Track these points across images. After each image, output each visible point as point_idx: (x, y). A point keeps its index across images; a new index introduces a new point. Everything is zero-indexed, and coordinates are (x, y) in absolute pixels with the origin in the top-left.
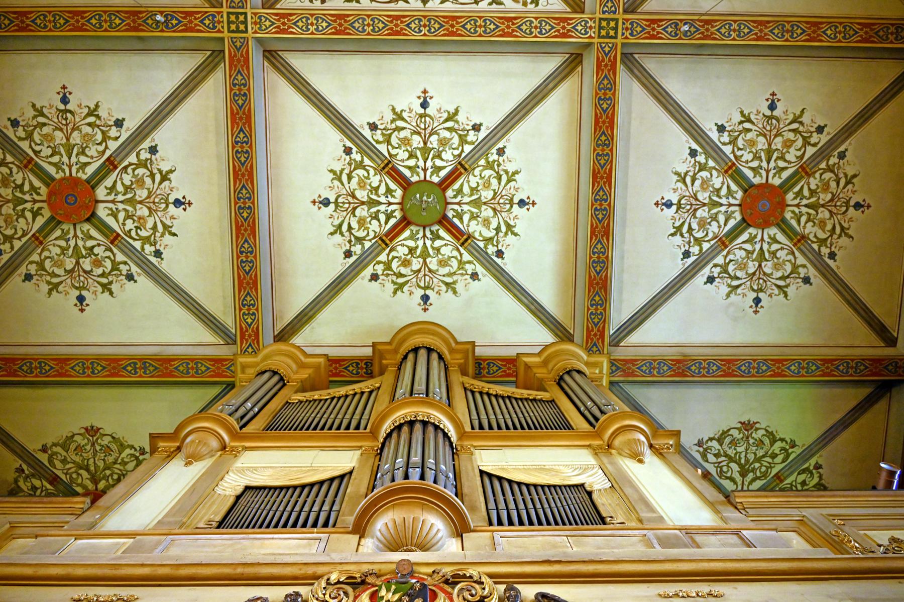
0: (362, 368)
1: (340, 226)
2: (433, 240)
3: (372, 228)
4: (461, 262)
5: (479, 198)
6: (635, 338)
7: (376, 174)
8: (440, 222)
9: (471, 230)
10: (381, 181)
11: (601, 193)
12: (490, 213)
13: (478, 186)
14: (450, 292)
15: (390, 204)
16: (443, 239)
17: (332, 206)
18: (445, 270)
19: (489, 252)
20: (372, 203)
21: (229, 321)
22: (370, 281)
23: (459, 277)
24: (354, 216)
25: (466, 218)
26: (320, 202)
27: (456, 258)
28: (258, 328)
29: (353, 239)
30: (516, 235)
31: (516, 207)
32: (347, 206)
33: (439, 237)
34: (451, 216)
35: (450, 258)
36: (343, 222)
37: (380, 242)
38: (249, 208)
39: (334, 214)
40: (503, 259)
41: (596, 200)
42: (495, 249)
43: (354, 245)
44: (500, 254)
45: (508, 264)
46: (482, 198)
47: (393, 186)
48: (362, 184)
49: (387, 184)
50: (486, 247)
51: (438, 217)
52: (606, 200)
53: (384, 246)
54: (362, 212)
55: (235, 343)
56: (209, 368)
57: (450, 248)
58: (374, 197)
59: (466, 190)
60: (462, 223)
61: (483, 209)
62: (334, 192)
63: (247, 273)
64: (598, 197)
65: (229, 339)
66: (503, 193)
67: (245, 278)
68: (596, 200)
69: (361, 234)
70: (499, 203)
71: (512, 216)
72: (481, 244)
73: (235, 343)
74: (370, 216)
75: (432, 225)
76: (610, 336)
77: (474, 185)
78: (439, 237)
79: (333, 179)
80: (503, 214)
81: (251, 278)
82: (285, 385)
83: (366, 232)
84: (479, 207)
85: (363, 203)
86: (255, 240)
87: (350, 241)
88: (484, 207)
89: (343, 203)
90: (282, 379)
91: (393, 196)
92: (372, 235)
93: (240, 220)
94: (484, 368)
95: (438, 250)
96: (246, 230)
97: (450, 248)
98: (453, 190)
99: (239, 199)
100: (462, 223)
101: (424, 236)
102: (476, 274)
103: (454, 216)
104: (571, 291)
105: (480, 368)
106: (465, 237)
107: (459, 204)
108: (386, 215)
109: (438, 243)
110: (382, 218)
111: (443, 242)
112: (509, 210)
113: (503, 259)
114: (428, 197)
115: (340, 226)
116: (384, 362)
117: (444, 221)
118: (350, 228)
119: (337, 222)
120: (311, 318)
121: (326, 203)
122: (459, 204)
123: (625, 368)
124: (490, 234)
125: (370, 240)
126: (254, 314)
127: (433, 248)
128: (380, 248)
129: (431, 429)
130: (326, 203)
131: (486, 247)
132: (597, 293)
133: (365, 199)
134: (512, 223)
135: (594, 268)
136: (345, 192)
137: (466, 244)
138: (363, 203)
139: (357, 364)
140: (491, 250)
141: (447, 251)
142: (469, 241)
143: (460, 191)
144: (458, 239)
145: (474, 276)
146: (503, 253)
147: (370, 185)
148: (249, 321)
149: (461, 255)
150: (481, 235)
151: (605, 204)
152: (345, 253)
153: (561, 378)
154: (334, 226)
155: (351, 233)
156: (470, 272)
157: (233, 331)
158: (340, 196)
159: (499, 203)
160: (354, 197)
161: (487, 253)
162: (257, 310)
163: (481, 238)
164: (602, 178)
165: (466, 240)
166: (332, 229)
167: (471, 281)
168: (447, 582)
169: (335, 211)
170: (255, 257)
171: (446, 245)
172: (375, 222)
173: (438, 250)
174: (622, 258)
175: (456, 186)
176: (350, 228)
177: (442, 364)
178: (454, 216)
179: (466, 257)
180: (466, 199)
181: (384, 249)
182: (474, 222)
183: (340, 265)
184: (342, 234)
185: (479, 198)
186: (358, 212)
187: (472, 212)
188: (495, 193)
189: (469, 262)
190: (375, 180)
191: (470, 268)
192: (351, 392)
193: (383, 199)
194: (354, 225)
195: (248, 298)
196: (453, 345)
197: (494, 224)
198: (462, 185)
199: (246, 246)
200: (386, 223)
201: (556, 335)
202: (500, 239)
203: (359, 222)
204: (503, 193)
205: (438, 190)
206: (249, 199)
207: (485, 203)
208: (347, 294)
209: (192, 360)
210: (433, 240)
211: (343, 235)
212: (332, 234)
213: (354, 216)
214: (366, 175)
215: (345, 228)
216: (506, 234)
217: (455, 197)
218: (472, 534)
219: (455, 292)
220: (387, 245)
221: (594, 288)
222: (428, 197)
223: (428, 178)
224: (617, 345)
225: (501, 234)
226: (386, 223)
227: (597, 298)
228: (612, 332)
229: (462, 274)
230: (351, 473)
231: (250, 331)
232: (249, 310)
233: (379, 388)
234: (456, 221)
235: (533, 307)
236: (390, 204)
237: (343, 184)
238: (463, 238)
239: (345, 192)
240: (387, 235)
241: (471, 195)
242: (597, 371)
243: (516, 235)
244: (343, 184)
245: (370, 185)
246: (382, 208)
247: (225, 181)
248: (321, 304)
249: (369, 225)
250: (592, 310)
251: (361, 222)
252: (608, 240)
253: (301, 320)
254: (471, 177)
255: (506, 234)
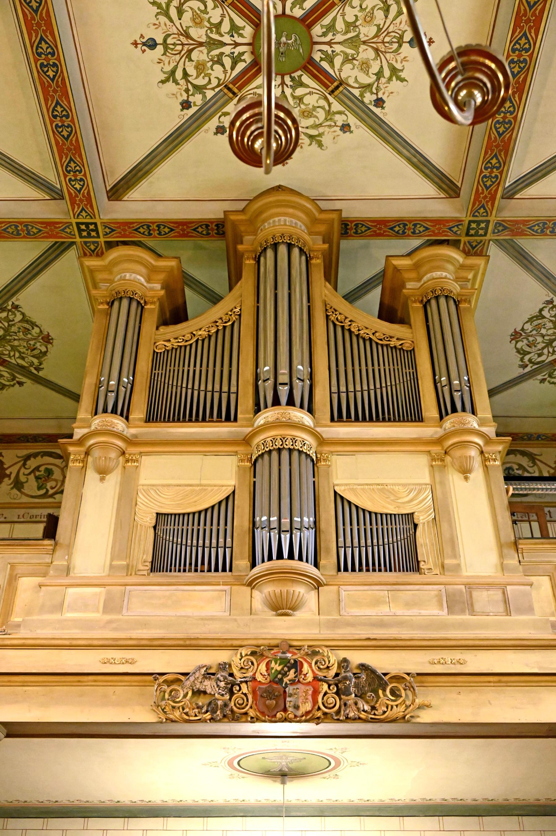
0: (212, 230)
1: (173, 72)
2: (294, 88)
3: (214, 74)
4: (328, 113)
5: (358, 36)
6: (533, 190)
7: (215, 7)
8: (305, 68)
9: (344, 75)
10: (223, 16)
11: (523, 41)
12: (371, 54)
13: (357, 20)
14: (314, 146)
15: (236, 45)
16: (307, 86)
17: (160, 49)
18: (310, 121)
19: (366, 100)
20: (212, 44)
21: (51, 177)
22: (216, 134)
23: (327, 129)
24: (191, 60)
25: (338, 61)
26: (144, 44)
27: (323, 108)
28: (89, 193)
29: (190, 87)
30: (403, 80)
31: (406, 46)
32: (179, 48)
33: (302, 84)
34: (318, 59)
35: (315, 108)
36: (176, 67)
37: (226, 91)
38: (54, 65)
39: (163, 58)
40: (383, 108)
41: (514, 51)
42: (374, 97)
43: (192, 95)
44: (379, 102)
45: (389, 115)
46: (361, 36)
47: (239, 21)
48: (197, 21)
49: (231, 20)
50: (362, 95)
51: (303, 62)
52: (527, 50)
53: (231, 95)
54: (200, 55)
55: (62, 198)
56: (40, 231)
57: (316, 97)
58: (215, 36)
59: (340, 25)
60: (333, 67)
61: (361, 50)
62: (160, 30)
63: (67, 139)
64: (517, 46)
65: (56, 195)
66: (391, 29)
67: (64, 144)
68: (514, 51)
69: (201, 82)
70: (383, 42)
71: (399, 58)
72: (356, 92)
73: (62, 198)
74: (212, 60)
75: (293, 73)
76: (505, 189)
77: (350, 18)
78: (302, 84)
79: (158, 14)
80: (388, 55)
81: (71, 143)
82: (143, 308)
83: (207, 79)
84: (356, 48)
85: (201, 44)
86: (69, 103)
87: (187, 91)
88: (363, 47)
89: (174, 44)
90: (139, 303)
91: (241, 35)
92: (214, 82)
93: (45, 80)
94: (352, 228)
95: (300, 99)
96: (55, 91)
97: (316, 97)
98: (322, 26)
99: (39, 54)
100: (333, 67)
101: (283, 83)
102: (348, 125)
103: (322, 59)
104: (465, 144)
105: (347, 229)
106: (336, 84)
107: (329, 43)
108: (233, 58)
109: (300, 91)
110: (227, 62)
111: (308, 90)
112: (396, 51)
113: (383, 108)
114: (288, 37)
115: (173, 72)
116: (240, 247)
117: (311, 66)
118: (186, 75)
119: (168, 68)
120: (147, 173)
121: (152, 44)
122: (329, 43)
123: (513, 228)
124: (365, 80)
125: (213, 89)
126: (81, 180)
127: (294, 97)
128: (226, 97)
129: (295, 454)
130: (152, 44)
131: (362, 95)
132: (496, 156)
133: (203, 39)
134: (398, 66)
135: (496, 129)
136: (175, 31)
137: (336, 93)
138: (201, 44)
139: (207, 226)
140: (369, 98)
141: (311, 100)
142: (341, 89)
143: (331, 28)
144: (327, 87)
145: (346, 128)
146: (384, 102)
147: (209, 21)
148: (78, 186)
149: (330, 105)
150: (356, 80)
151: (525, 56)
152: (182, 104)
153: (429, 301)
154: (164, 73)
155: (188, 81)
156: (340, 123)
157: (58, 186)
158: (169, 35)
159: (383, 42)
160: (188, 36)
161: (363, 102)
162: (85, 175)
163: (357, 86)
164: (528, 21)
165: (337, 87)
166: (163, 77)
167: (341, 133)
168: (307, 654)
169: (164, 54)
170: (73, 121)
171: (310, 93)
172: (217, 67)
173: (300, 99)
174: (538, 104)
175: (327, 21)
176: (186, 75)
177: (304, 258)
178: (322, 59)
179: (336, 106)
180: (340, 38)
181: (232, 99)
182: (348, 66)
183: (176, 118)
184: (176, 82)
185: (358, 36)
186: (194, 55)
187: (345, 54)
188: (379, 29)
189: (340, 113)
190: (215, 15)
191: (340, 120)
192: (214, 330)
193: (227, 39)
194: (191, 70)
195: (73, 165)
196: (317, 214)
197: (375, 69)
198: (334, 19)
199: (59, 109)
200: (233, 68)
201: (440, 188)
202: (381, 86)
203: (196, 67)
204: (391, 29)
205: (301, 28)
206: (53, 54)
207: (364, 42)
208: (188, 149)
209: (21, 223)
210: (294, 88)
211: (177, 84)
212: (163, 82)
213: (191, 60)
214: (202, 8)
215: (179, 74)
216: (390, 79)
217: (324, 35)
218: (325, 587)
219: (320, 145)
220: (234, 94)
221: (492, 151)
222: (288, 37)
223: (288, 12)
224: (511, 197)
225: (383, 80)
226: (233, 68)
227: (494, 161)
228: (507, 184)
229: (330, 126)
230: (234, 492)
231: (81, 196)
232: (75, 176)
233: (240, 315)
234: (325, 65)
235: (415, 160)
236: (236, 45)
237: (171, 21)
238: (333, 85)
239: (175, 31)
240: (234, 82)
241: (347, 32)
242: (470, 276)
243: (403, 80)
244: (171, 21)
245: (209, 21)
246: (227, 50)
247: (22, 57)
248: (158, 158)
249: (210, 71)
250: (486, 173)
251: (200, 68)
252: (520, 99)
253: (135, 175)
254: (348, 9)
255: (390, 79)
